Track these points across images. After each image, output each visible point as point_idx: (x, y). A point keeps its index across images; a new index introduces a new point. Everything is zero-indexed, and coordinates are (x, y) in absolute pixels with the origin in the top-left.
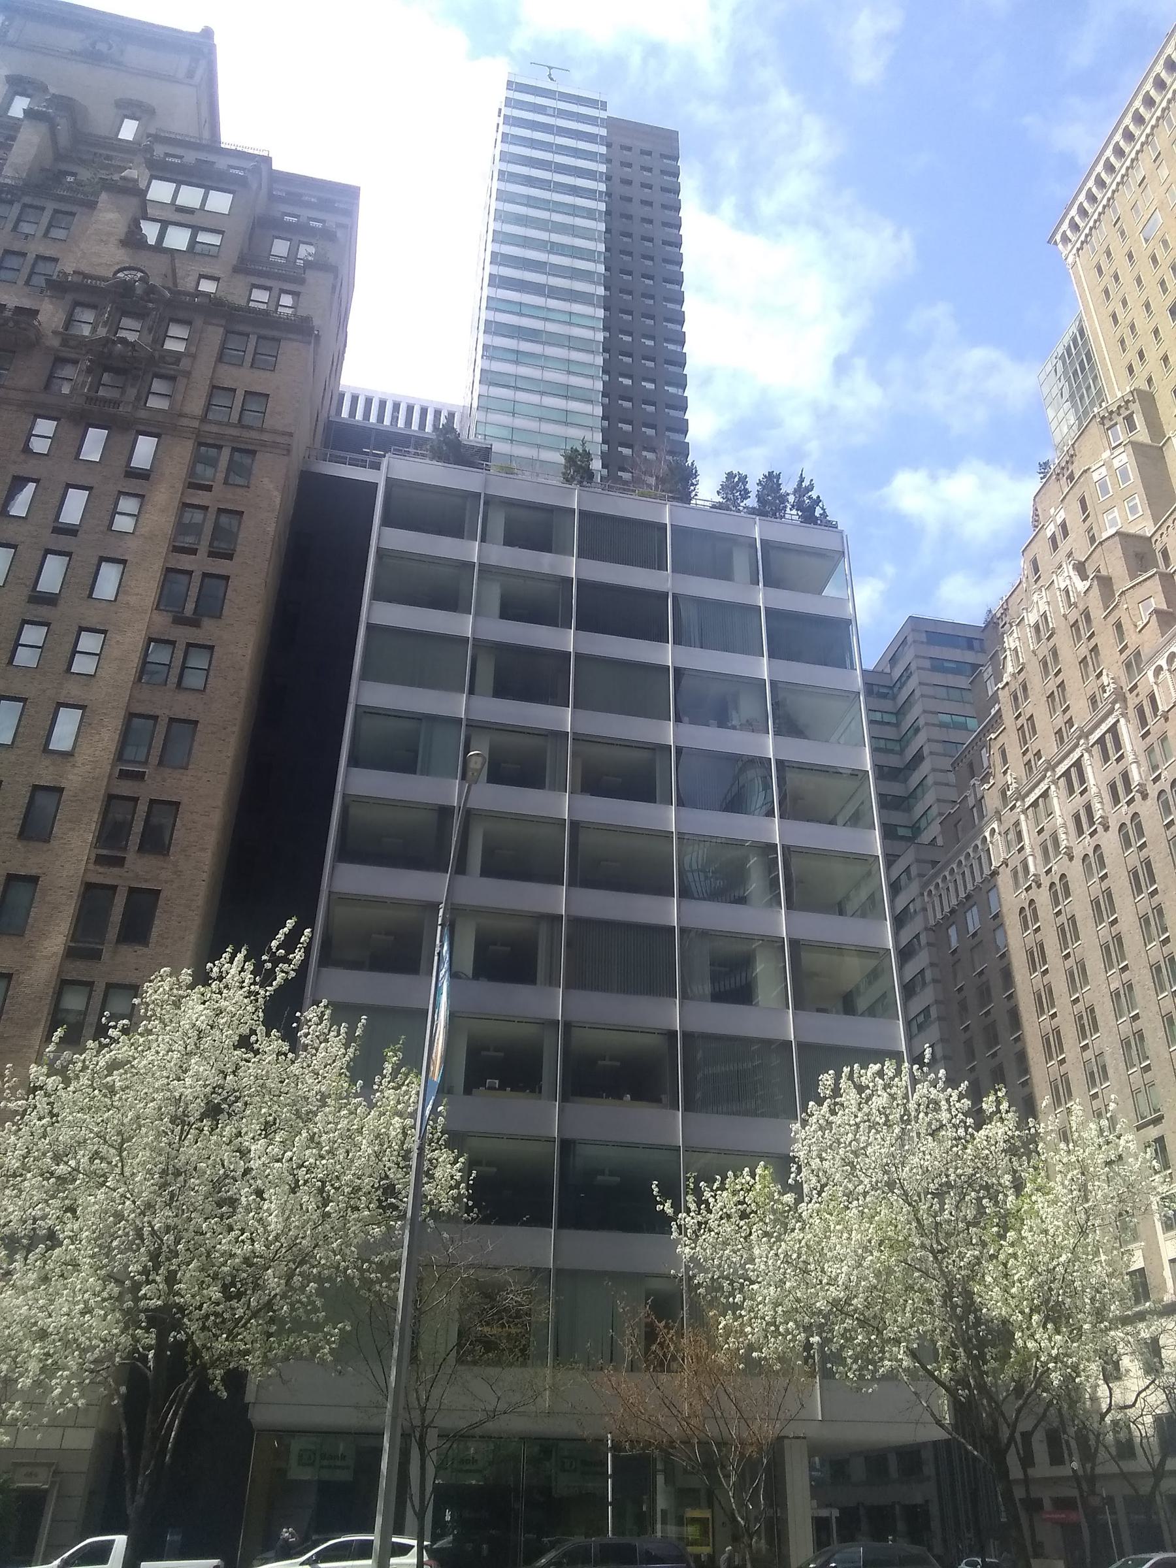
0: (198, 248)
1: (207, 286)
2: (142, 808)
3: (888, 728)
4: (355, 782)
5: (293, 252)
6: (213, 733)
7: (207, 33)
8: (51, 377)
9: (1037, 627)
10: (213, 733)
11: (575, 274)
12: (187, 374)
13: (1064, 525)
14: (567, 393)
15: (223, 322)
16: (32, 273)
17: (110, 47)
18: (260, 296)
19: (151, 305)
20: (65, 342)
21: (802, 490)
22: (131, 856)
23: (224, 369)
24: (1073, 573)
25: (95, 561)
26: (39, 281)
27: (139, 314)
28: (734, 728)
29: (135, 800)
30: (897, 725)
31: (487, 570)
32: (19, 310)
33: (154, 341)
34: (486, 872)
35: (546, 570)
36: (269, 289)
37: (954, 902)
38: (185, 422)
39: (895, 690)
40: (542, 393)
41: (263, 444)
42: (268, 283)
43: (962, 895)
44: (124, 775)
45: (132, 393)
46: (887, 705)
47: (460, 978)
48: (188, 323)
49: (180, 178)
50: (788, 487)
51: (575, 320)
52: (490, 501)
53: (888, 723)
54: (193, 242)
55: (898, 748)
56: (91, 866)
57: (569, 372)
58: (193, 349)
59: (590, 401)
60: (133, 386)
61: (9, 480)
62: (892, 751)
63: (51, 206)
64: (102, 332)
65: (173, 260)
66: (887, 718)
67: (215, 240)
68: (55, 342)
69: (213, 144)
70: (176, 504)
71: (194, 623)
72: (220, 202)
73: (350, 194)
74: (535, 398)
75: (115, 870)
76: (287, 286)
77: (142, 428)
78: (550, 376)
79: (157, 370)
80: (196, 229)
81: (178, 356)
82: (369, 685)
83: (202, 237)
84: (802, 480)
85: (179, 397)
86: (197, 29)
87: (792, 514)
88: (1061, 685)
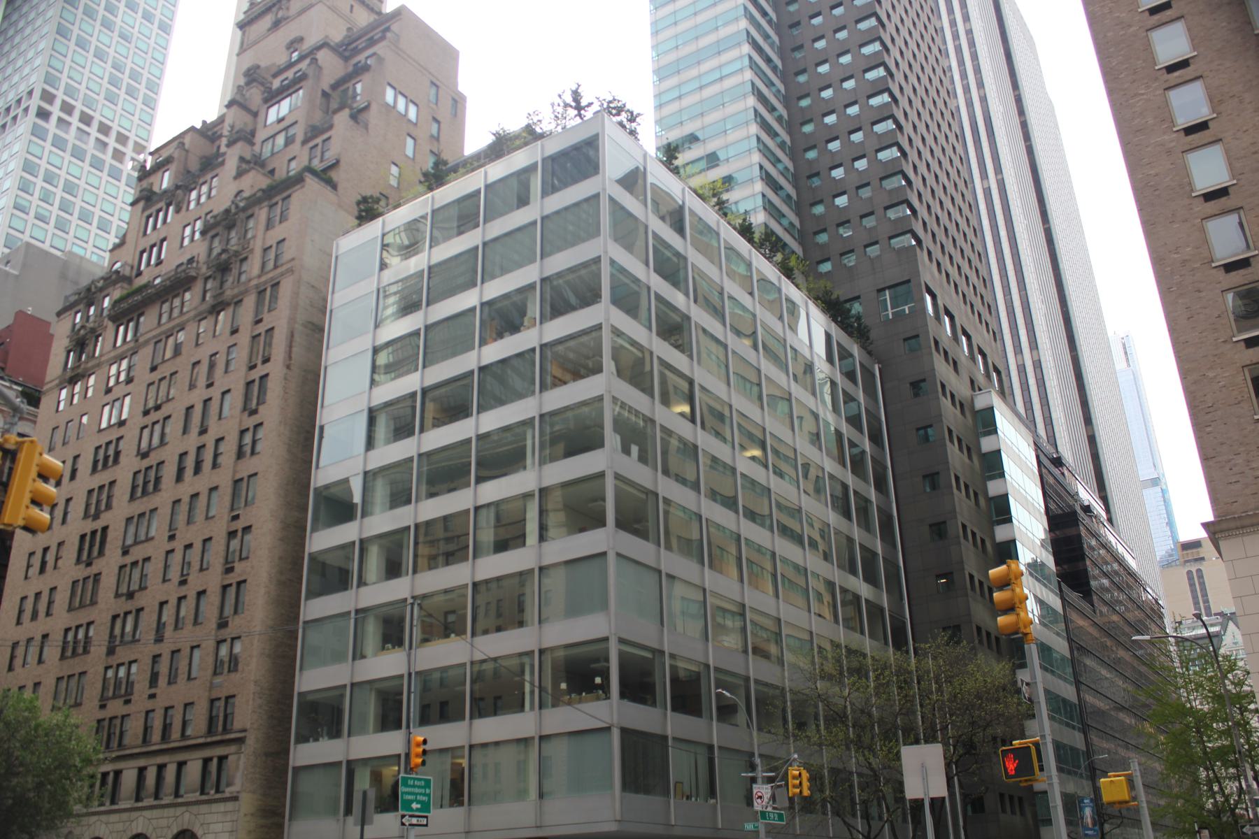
15: (266, 203)
22: (236, 565)
23: (271, 233)
25: (219, 396)
29: (236, 531)
41: (282, 274)
48: (252, 216)
68: (204, 269)
75: (231, 575)
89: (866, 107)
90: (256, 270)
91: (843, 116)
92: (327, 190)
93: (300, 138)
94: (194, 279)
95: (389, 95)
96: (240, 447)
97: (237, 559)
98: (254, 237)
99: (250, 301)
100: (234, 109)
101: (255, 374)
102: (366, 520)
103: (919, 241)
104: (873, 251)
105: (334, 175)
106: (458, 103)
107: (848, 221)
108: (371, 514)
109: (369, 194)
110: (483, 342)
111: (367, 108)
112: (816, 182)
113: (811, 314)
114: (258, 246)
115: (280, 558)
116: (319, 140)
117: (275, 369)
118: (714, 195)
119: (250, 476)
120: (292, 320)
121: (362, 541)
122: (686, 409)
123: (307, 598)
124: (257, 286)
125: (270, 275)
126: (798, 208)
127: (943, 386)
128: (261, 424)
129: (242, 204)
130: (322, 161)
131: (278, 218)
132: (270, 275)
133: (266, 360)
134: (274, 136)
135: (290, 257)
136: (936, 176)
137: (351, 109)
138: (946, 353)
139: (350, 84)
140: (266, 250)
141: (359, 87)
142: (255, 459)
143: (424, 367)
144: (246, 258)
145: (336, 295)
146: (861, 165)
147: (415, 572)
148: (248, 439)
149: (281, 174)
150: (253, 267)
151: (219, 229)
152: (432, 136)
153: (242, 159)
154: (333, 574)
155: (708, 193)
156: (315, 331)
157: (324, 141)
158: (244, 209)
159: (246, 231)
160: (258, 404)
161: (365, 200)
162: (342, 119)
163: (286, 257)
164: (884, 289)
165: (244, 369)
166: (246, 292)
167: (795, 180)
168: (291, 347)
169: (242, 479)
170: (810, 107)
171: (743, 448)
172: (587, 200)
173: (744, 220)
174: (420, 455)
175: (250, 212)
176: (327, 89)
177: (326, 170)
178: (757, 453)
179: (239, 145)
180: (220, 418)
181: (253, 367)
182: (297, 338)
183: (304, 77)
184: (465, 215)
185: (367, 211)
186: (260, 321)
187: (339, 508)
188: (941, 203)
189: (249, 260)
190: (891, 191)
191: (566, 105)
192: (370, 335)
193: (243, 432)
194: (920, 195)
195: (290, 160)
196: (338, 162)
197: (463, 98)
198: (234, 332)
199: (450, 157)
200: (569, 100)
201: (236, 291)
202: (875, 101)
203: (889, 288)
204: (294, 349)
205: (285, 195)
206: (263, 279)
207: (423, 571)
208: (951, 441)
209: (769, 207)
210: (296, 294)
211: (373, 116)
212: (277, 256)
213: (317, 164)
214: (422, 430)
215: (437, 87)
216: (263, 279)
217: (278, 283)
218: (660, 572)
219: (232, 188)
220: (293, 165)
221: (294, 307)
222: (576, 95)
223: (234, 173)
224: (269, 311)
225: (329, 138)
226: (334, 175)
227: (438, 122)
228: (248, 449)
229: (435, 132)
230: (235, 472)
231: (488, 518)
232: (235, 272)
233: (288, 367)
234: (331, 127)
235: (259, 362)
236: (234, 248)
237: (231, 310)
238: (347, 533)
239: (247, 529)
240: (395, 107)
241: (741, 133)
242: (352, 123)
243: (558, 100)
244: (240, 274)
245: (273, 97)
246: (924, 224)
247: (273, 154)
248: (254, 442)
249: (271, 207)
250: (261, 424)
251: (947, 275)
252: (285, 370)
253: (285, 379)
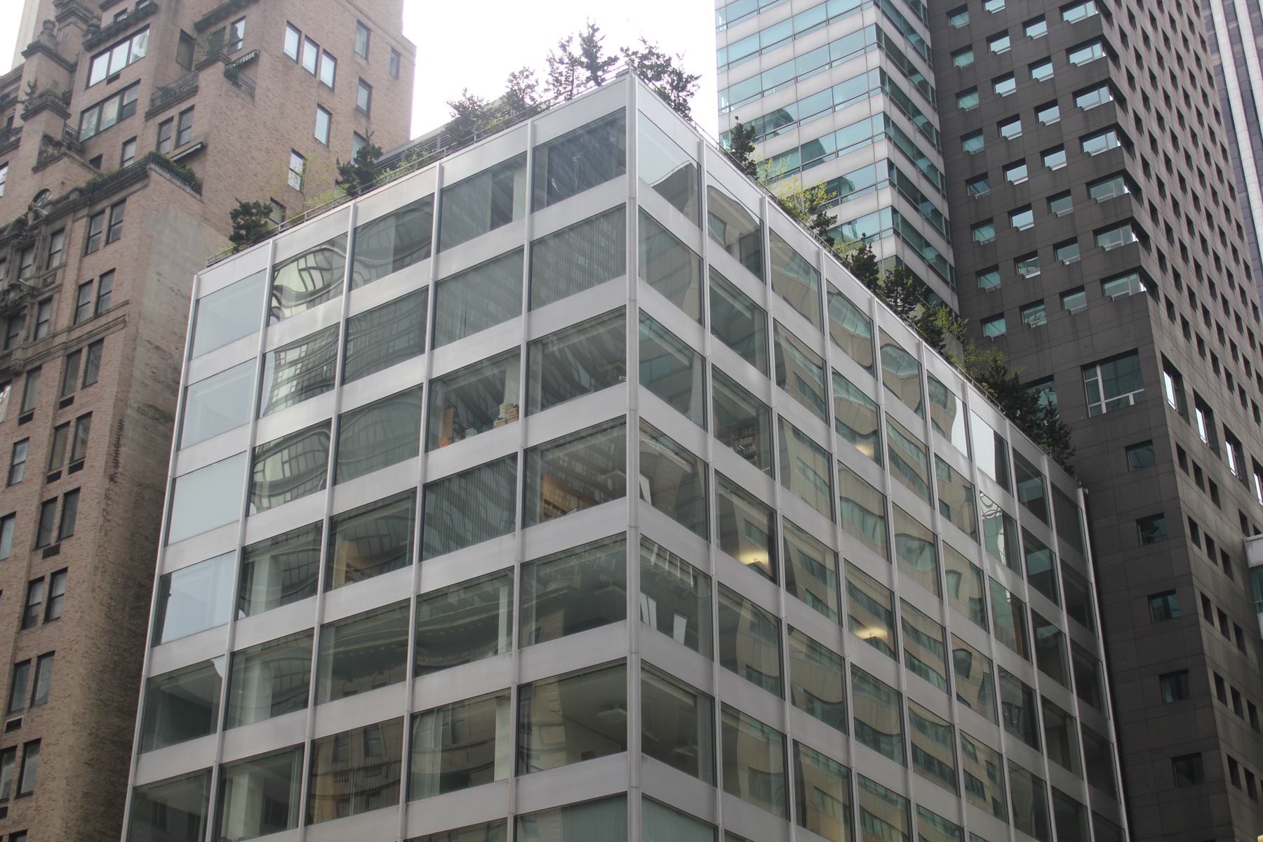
15: (85, 212)
22: (10, 805)
23: (90, 260)
29: (15, 748)
33: (39, 268)
41: (108, 327)
48: (61, 231)
49: (111, 43)
71: (54, 551)
72: (138, 46)
77: (29, 367)
89: (1065, 68)
90: (64, 320)
91: (1026, 82)
92: (185, 194)
93: (143, 107)
95: (290, 42)
96: (28, 608)
97: (13, 795)
98: (63, 266)
99: (52, 371)
100: (38, 58)
101: (58, 490)
102: (231, 733)
103: (1152, 287)
104: (1075, 302)
105: (196, 168)
106: (400, 57)
107: (1034, 254)
108: (241, 723)
109: (252, 201)
110: (432, 443)
111: (253, 62)
112: (982, 189)
113: (970, 406)
114: (69, 282)
115: (86, 794)
116: (174, 112)
117: (91, 481)
118: (812, 210)
119: (40, 658)
120: (121, 402)
121: (222, 768)
122: (762, 558)
124: (66, 345)
125: (88, 328)
126: (952, 232)
127: (1193, 526)
128: (65, 570)
129: (45, 212)
130: (178, 145)
131: (103, 237)
132: (88, 328)
133: (76, 467)
134: (100, 104)
135: (122, 300)
136: (1182, 180)
137: (228, 62)
138: (1198, 471)
139: (227, 23)
140: (81, 287)
141: (241, 27)
142: (51, 627)
143: (335, 482)
144: (49, 300)
145: (194, 363)
146: (1056, 161)
147: (309, 820)
148: (40, 595)
149: (111, 165)
150: (60, 314)
152: (358, 109)
153: (47, 139)
155: (803, 207)
156: (158, 420)
157: (182, 114)
158: (49, 220)
159: (51, 256)
160: (60, 538)
161: (245, 209)
162: (211, 79)
163: (114, 299)
164: (1092, 366)
165: (39, 480)
166: (48, 354)
167: (947, 187)
168: (118, 445)
169: (28, 661)
170: (971, 67)
171: (857, 623)
172: (605, 215)
173: (862, 251)
174: (323, 627)
175: (57, 225)
176: (189, 31)
177: (183, 160)
178: (879, 632)
179: (45, 116)
181: (53, 478)
182: (129, 432)
184: (408, 237)
185: (249, 228)
186: (70, 402)
187: (189, 708)
188: (1190, 223)
189: (54, 304)
190: (1105, 204)
191: (574, 62)
192: (250, 428)
193: (32, 584)
194: (1153, 211)
195: (126, 144)
196: (204, 147)
197: (410, 49)
198: (26, 418)
199: (386, 144)
200: (577, 50)
201: (30, 353)
202: (1079, 58)
203: (1102, 362)
204: (123, 449)
206: (76, 334)
207: (322, 819)
208: (1208, 617)
209: (903, 230)
210: (129, 360)
211: (263, 76)
212: (99, 297)
213: (168, 149)
214: (328, 587)
215: (368, 30)
216: (76, 334)
217: (102, 340)
218: (715, 828)
219: (30, 186)
220: (131, 150)
221: (126, 382)
222: (590, 46)
224: (84, 386)
225: (191, 108)
226: (196, 168)
227: (369, 87)
228: (40, 612)
229: (362, 102)
230: (16, 649)
231: (431, 734)
232: (30, 321)
233: (112, 478)
234: (194, 91)
235: (65, 469)
236: (31, 283)
237: (21, 382)
238: (200, 753)
239: (32, 746)
240: (298, 60)
241: (859, 110)
242: (228, 85)
243: (559, 53)
244: (38, 325)
245: (101, 42)
246: (1161, 257)
247: (98, 133)
248: (51, 601)
249: (92, 217)
250: (65, 570)
251: (1200, 342)
252: (107, 483)
253: (107, 497)
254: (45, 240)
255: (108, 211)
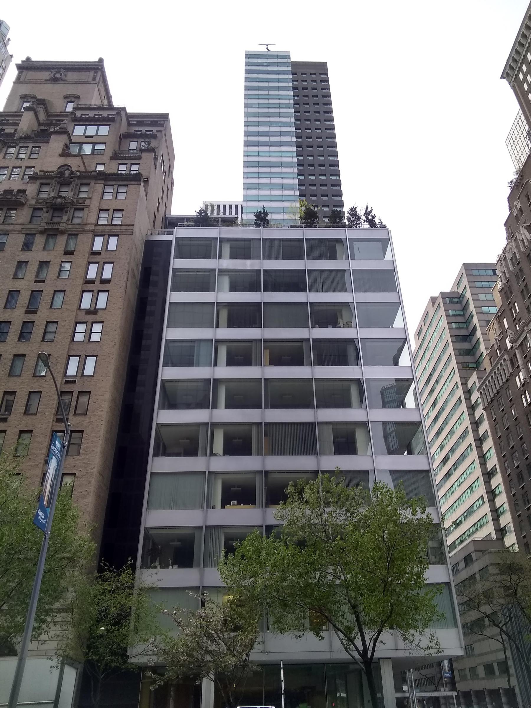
0: (96, 152)
1: (100, 168)
2: (75, 395)
3: (459, 317)
4: (168, 373)
5: (139, 146)
6: (104, 359)
7: (101, 60)
8: (32, 217)
9: (512, 259)
10: (104, 359)
11: (282, 134)
12: (88, 207)
13: (520, 210)
14: (283, 187)
15: (103, 182)
16: (24, 174)
17: (61, 75)
18: (123, 168)
19: (72, 180)
20: (37, 202)
21: (367, 213)
22: (70, 417)
24: (526, 232)
26: (26, 177)
27: (68, 184)
28: (340, 327)
29: (72, 392)
30: (464, 315)
31: (222, 272)
32: (19, 191)
34: (228, 406)
35: (248, 267)
36: (126, 164)
37: (492, 396)
38: (88, 227)
39: (461, 299)
40: (271, 189)
42: (126, 162)
43: (495, 392)
44: (67, 382)
45: (65, 218)
46: (458, 307)
47: (216, 455)
48: (88, 184)
49: (87, 123)
50: (361, 212)
51: (283, 154)
52: (222, 240)
53: (460, 315)
54: (93, 149)
55: (465, 326)
56: (54, 423)
57: (282, 178)
58: (90, 196)
59: (294, 189)
60: (66, 215)
61: (16, 263)
62: (462, 328)
63: (31, 145)
64: (52, 194)
65: (82, 159)
66: (459, 313)
67: (102, 147)
68: (33, 202)
69: (110, 107)
70: (86, 262)
72: (104, 130)
73: (165, 117)
74: (268, 192)
76: (133, 162)
77: (70, 233)
78: (274, 181)
79: (76, 207)
80: (94, 144)
81: (84, 200)
82: (170, 329)
83: (97, 147)
84: (367, 209)
85: (85, 217)
86: (97, 60)
87: (366, 225)
88: (526, 286)
94: (22, 205)
123: (155, 455)
129: (78, 174)
151: (53, 182)
154: (189, 442)
158: (79, 178)
180: (51, 307)
183: (113, 120)
201: (70, 227)
205: (126, 183)
216: (98, 228)
219: (61, 161)
223: (60, 152)
232: (70, 214)
249: (105, 185)
254: (77, 185)
255: (116, 186)
